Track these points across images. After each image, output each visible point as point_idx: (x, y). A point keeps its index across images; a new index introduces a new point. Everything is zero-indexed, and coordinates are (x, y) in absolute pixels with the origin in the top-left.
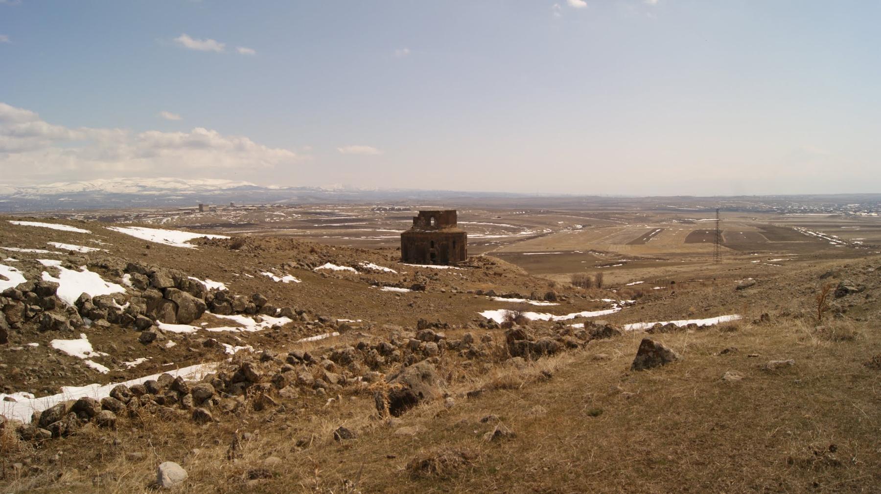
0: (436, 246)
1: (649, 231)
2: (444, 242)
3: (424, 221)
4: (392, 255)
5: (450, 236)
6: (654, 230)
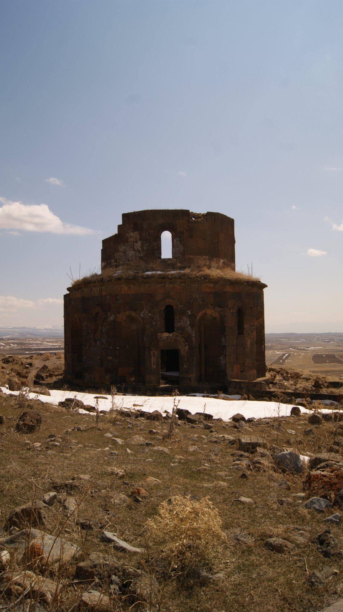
0: (183, 322)
1: (281, 355)
2: (209, 312)
3: (138, 245)
4: (47, 363)
5: (229, 289)
6: (284, 355)
